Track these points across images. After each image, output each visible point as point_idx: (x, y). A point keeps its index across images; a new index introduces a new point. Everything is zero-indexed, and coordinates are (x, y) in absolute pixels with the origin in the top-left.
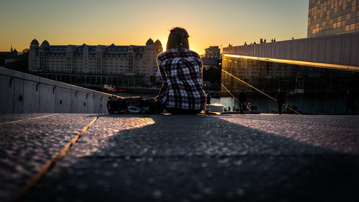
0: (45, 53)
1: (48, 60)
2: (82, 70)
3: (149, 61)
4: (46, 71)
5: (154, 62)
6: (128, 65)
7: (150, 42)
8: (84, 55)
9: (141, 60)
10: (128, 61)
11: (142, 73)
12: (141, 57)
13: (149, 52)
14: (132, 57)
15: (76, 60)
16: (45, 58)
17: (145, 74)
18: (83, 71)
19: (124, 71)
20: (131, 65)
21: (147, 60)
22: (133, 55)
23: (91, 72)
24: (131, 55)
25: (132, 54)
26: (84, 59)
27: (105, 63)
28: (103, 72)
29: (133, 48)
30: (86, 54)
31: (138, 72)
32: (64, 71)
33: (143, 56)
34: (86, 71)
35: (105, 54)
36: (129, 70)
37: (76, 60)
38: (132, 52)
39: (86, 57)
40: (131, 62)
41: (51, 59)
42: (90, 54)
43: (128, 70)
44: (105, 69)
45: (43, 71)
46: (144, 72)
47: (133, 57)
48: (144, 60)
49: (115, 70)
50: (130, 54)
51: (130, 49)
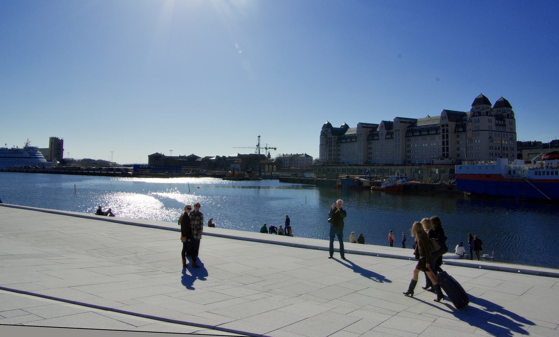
0: (335, 138)
5: (490, 137)
7: (482, 101)
12: (464, 130)
13: (478, 120)
14: (447, 131)
15: (370, 146)
20: (445, 146)
22: (449, 128)
24: (445, 128)
25: (447, 125)
27: (408, 146)
33: (468, 128)
35: (408, 131)
36: (443, 155)
37: (370, 146)
42: (387, 134)
44: (408, 157)
47: (449, 131)
48: (469, 134)
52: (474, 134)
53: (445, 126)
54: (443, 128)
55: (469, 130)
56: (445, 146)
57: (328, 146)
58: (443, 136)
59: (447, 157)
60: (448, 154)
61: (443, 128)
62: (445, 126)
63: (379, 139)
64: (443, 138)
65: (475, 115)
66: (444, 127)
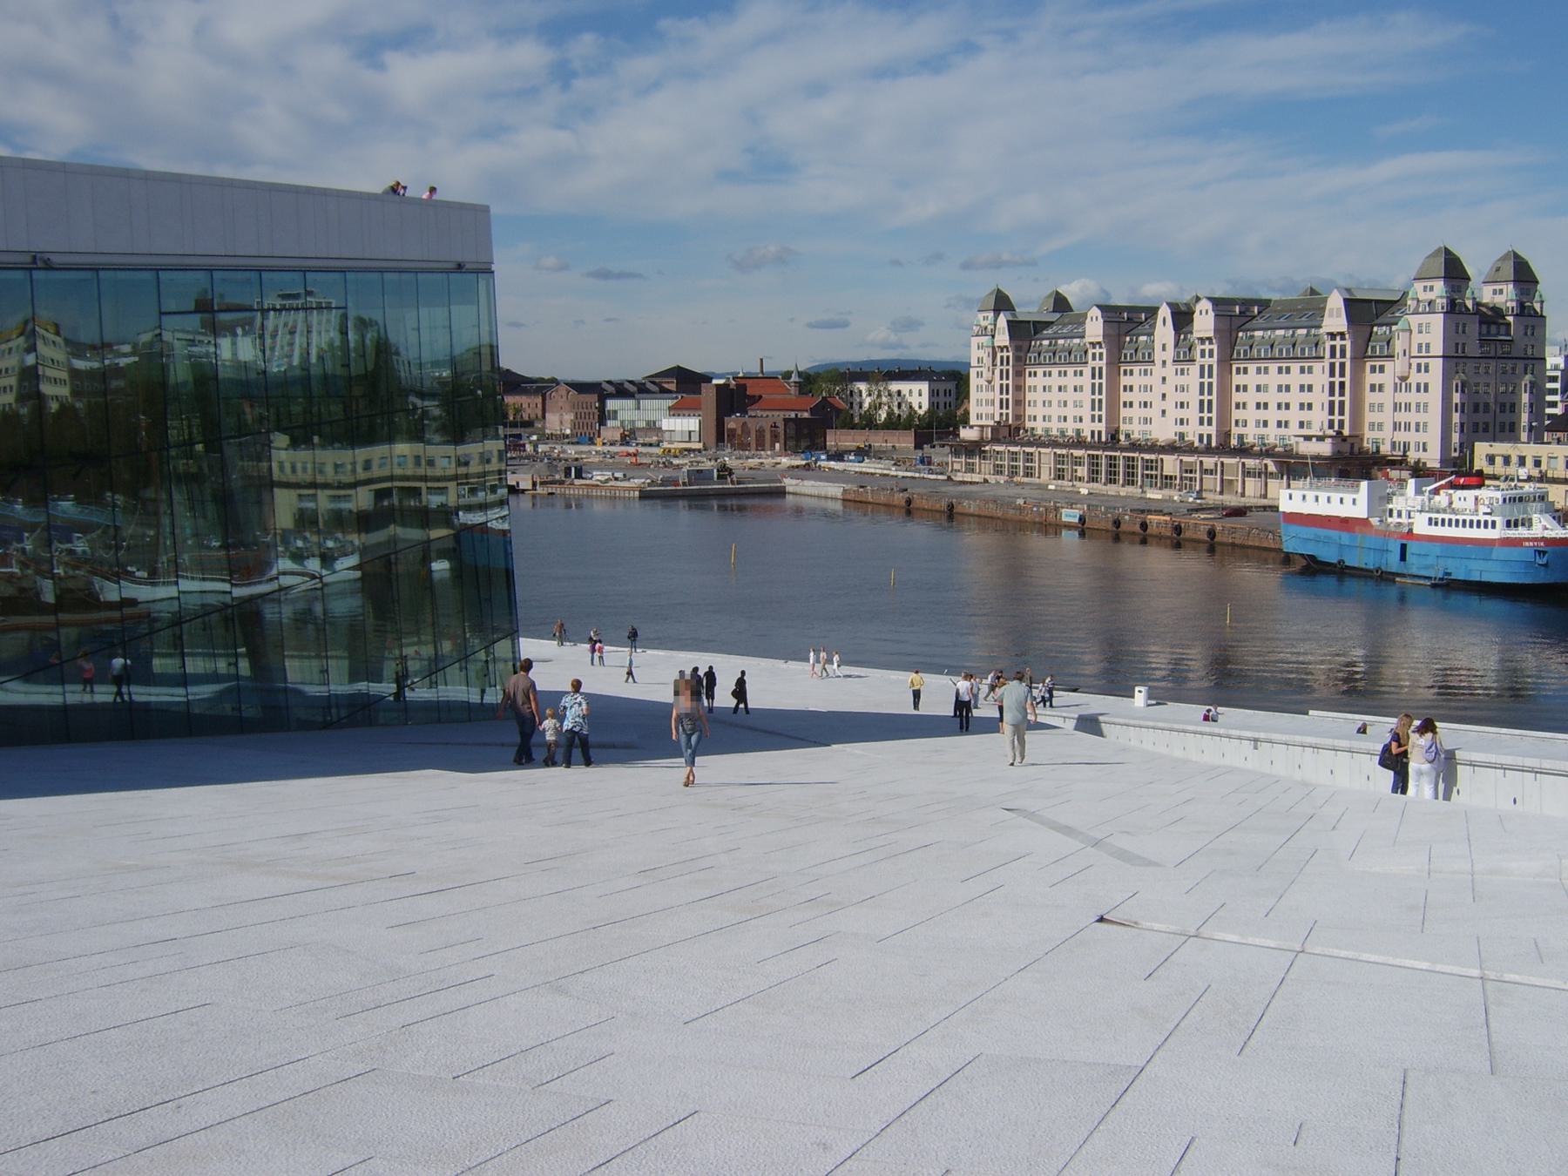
2: (1147, 427)
3: (1427, 370)
6: (1326, 398)
8: (1159, 356)
9: (1388, 365)
10: (1326, 379)
11: (1393, 444)
18: (1154, 436)
20: (1337, 398)
21: (1419, 365)
23: (1182, 435)
25: (1342, 335)
26: (1157, 369)
30: (1164, 348)
32: (1070, 433)
39: (1164, 362)
40: (1337, 379)
43: (1326, 425)
46: (1401, 437)
49: (1279, 424)
50: (1332, 336)
51: (1331, 315)
52: (1414, 367)
53: (1338, 338)
54: (1333, 343)
55: (1401, 354)
56: (1337, 398)
57: (997, 372)
58: (1332, 366)
60: (1341, 423)
61: (1333, 343)
62: (1338, 338)
63: (1153, 361)
64: (1332, 374)
65: (1420, 310)
66: (1335, 340)
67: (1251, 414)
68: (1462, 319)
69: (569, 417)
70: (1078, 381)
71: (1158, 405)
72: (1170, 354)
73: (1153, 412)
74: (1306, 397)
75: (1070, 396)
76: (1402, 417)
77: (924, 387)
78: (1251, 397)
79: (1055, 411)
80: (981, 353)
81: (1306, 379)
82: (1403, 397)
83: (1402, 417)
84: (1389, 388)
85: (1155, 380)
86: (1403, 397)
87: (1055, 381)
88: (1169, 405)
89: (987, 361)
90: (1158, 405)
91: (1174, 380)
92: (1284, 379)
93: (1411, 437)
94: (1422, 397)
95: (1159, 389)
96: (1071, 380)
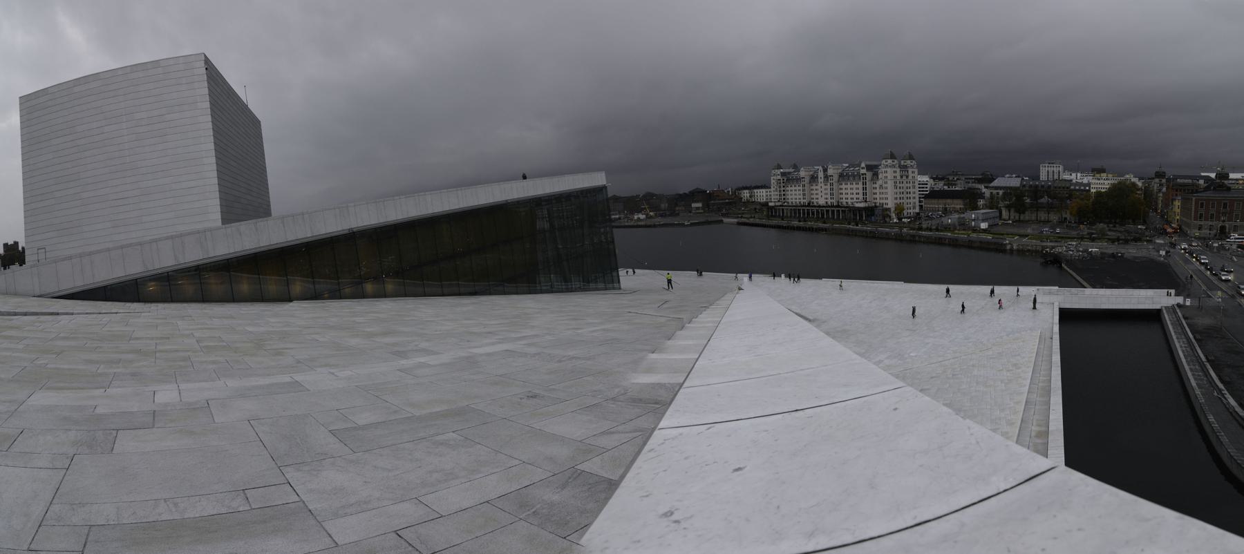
1: (787, 188)
4: (786, 204)
6: (862, 191)
8: (820, 180)
16: (784, 187)
17: (883, 204)
19: (855, 200)
23: (826, 202)
25: (865, 174)
26: (820, 185)
28: (838, 202)
29: (866, 166)
31: (875, 201)
33: (880, 177)
34: (822, 202)
38: (864, 171)
41: (789, 188)
45: (780, 203)
46: (881, 202)
50: (863, 174)
59: (866, 201)
67: (844, 196)
68: (895, 169)
69: (667, 205)
70: (799, 188)
71: (820, 194)
72: (822, 180)
73: (819, 196)
74: (857, 191)
75: (797, 192)
76: (881, 196)
77: (747, 191)
78: (844, 191)
79: (794, 197)
80: (774, 181)
81: (857, 186)
82: (882, 191)
83: (881, 196)
84: (878, 188)
85: (818, 187)
86: (882, 191)
87: (793, 188)
88: (823, 194)
89: (776, 183)
90: (820, 194)
91: (824, 187)
92: (852, 186)
93: (884, 201)
94: (886, 191)
95: (820, 190)
96: (797, 188)
